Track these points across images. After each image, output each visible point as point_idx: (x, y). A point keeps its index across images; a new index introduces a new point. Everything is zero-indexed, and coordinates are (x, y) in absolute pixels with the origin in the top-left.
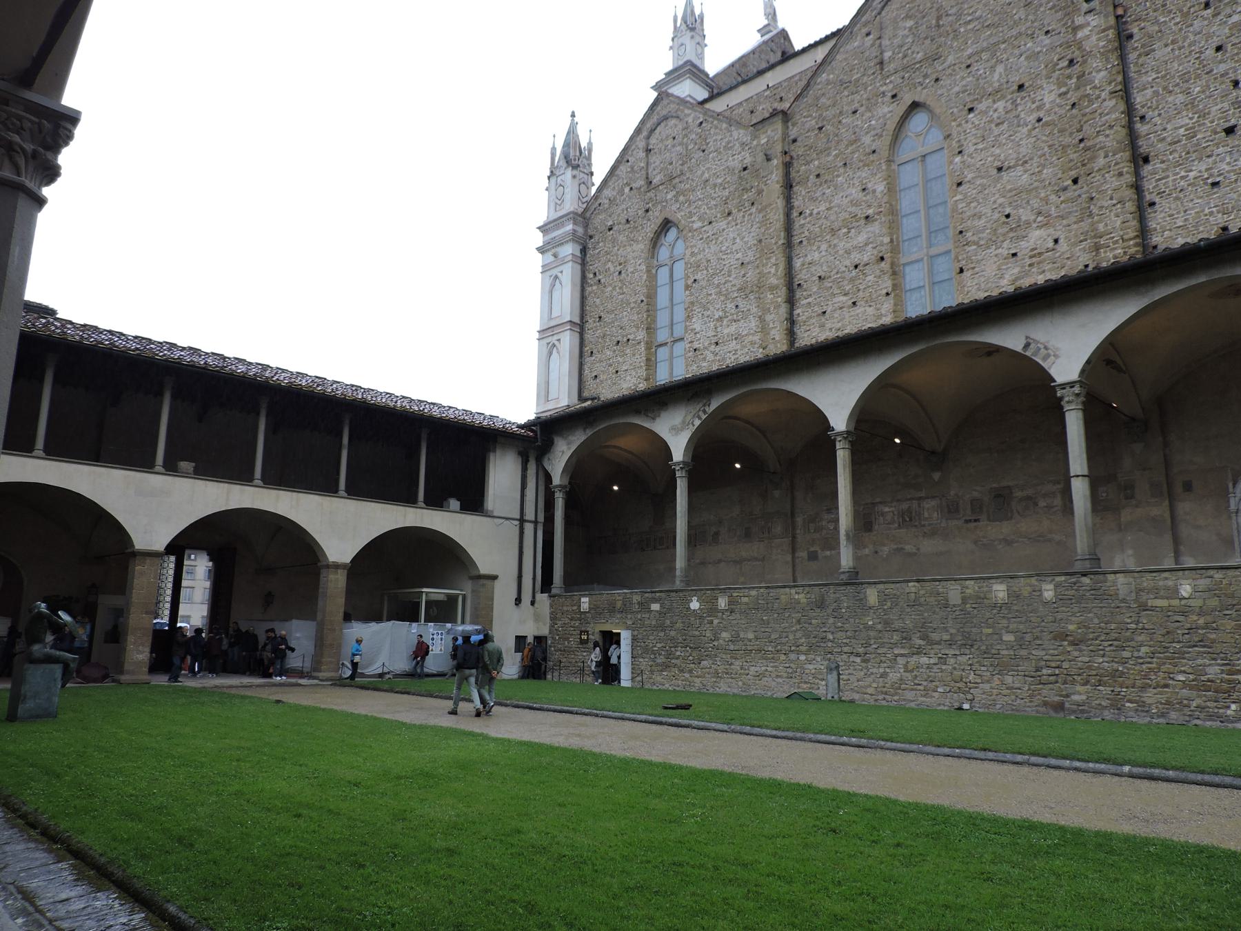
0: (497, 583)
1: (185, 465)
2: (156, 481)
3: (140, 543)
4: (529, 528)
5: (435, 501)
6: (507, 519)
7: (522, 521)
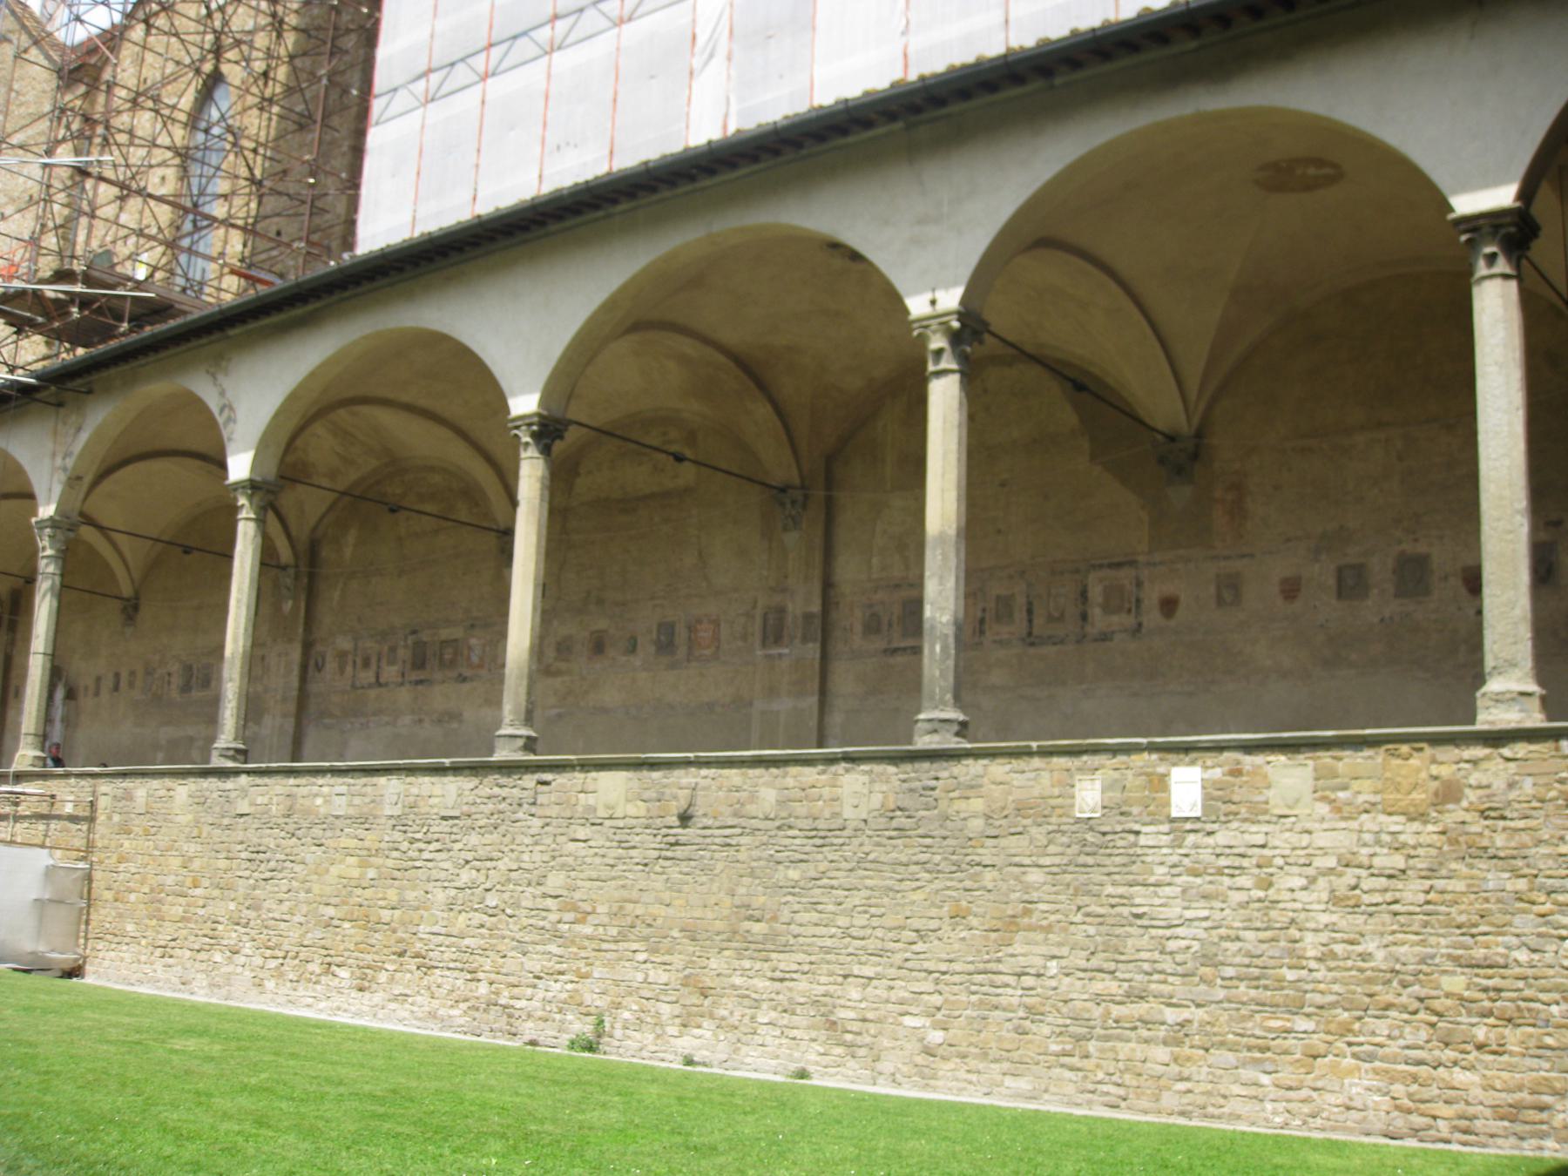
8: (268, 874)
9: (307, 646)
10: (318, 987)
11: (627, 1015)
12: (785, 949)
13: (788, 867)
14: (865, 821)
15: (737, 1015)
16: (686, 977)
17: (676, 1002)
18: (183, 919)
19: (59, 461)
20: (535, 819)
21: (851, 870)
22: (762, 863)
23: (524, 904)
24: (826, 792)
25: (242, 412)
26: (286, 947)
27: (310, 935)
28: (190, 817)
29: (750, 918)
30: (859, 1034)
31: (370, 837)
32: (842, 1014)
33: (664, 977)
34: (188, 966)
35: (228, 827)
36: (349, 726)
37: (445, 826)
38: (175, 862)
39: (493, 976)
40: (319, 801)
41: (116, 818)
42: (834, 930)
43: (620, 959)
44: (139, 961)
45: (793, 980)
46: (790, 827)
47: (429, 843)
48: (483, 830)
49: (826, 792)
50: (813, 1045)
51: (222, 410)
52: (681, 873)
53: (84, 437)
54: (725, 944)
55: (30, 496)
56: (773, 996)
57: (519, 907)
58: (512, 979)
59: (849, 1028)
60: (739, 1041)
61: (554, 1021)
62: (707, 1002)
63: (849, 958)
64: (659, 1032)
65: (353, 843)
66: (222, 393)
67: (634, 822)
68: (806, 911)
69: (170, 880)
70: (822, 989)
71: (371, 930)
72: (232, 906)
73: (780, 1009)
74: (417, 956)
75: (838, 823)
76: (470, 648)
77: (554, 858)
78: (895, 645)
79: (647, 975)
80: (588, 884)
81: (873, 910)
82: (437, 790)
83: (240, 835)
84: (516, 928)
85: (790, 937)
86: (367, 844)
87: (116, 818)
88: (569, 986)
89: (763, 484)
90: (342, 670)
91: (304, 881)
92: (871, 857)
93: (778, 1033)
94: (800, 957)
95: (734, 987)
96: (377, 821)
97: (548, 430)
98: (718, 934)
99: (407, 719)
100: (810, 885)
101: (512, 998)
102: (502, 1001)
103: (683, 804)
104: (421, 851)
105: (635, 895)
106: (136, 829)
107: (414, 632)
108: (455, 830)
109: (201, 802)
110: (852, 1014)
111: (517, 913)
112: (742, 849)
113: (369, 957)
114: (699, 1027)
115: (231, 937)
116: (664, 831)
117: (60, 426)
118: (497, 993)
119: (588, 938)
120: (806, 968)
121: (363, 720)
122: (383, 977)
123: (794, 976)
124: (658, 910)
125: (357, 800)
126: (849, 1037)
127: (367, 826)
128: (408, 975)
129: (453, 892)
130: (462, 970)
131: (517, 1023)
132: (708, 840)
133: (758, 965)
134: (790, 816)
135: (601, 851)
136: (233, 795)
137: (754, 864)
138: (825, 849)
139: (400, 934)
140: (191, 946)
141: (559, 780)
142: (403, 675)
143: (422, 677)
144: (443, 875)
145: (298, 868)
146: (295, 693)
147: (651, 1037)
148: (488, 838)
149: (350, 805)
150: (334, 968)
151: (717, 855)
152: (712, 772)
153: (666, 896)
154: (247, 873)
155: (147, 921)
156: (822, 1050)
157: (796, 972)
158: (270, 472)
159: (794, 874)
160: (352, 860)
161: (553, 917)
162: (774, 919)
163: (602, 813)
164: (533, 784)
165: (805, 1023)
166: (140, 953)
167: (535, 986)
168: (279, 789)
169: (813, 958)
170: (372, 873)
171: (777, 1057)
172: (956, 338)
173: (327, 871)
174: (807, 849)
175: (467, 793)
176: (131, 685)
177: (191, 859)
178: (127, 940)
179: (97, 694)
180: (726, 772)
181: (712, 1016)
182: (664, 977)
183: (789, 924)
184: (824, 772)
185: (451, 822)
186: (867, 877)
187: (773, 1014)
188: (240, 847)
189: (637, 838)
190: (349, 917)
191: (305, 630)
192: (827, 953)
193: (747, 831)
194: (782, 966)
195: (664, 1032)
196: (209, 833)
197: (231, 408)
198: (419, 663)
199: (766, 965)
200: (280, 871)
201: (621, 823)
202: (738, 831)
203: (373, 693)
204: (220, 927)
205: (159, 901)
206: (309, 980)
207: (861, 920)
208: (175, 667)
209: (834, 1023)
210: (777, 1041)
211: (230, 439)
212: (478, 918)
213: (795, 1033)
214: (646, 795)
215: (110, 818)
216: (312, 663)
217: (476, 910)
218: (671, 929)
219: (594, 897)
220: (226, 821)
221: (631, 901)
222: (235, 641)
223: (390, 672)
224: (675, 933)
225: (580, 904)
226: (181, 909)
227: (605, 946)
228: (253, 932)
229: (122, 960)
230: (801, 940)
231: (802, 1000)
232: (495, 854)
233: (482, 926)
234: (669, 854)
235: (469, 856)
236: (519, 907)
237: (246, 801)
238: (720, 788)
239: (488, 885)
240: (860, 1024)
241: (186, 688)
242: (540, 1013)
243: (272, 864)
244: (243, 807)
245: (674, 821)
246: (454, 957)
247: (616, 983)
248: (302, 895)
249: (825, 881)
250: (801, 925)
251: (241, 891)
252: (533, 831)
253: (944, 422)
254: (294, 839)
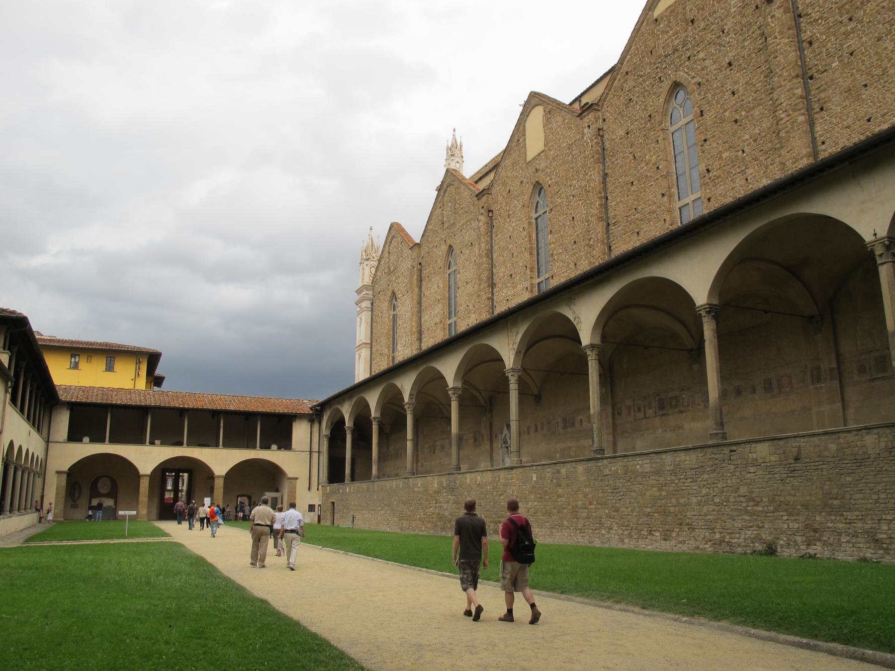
0: (297, 481)
1: (157, 442)
2: (146, 449)
3: (142, 472)
4: (315, 456)
5: (266, 446)
6: (303, 451)
7: (311, 452)
8: (620, 498)
9: (613, 406)
10: (647, 540)
11: (782, 542)
12: (850, 510)
13: (846, 476)
14: (879, 454)
15: (832, 539)
16: (807, 525)
17: (804, 535)
18: (587, 518)
19: (511, 347)
20: (731, 466)
21: (876, 475)
22: (834, 475)
23: (731, 500)
24: (859, 443)
25: (583, 318)
26: (631, 525)
27: (641, 520)
28: (585, 478)
29: (832, 498)
30: (890, 544)
31: (662, 480)
32: (880, 536)
33: (796, 526)
34: (591, 536)
35: (601, 480)
36: (635, 436)
37: (693, 472)
38: (581, 496)
39: (721, 530)
40: (638, 467)
41: (554, 481)
42: (871, 501)
43: (776, 519)
44: (571, 536)
45: (855, 523)
46: (845, 459)
47: (687, 479)
48: (709, 472)
49: (859, 443)
50: (869, 550)
51: (575, 319)
52: (798, 482)
53: (520, 336)
54: (822, 510)
55: (501, 360)
56: (847, 530)
57: (729, 502)
58: (729, 531)
59: (884, 542)
60: (834, 550)
61: (750, 546)
62: (817, 535)
63: (880, 512)
64: (797, 548)
65: (654, 482)
66: (574, 313)
67: (774, 463)
68: (857, 493)
69: (580, 503)
70: (869, 526)
71: (667, 516)
72: (607, 511)
73: (851, 536)
74: (688, 524)
75: (867, 456)
76: (683, 399)
77: (741, 481)
78: (874, 377)
79: (789, 525)
80: (758, 490)
81: (888, 491)
82: (688, 458)
83: (607, 483)
84: (729, 510)
85: (851, 505)
86: (661, 482)
87: (554, 481)
88: (755, 532)
89: (803, 316)
90: (629, 413)
91: (636, 499)
92: (884, 469)
93: (851, 545)
94: (857, 513)
95: (828, 527)
96: (664, 472)
97: (714, 311)
98: (818, 506)
99: (660, 431)
100: (858, 483)
101: (731, 538)
102: (726, 540)
103: (795, 454)
104: (684, 483)
105: (779, 493)
106: (563, 485)
107: (658, 395)
108: (697, 473)
109: (588, 471)
110: (885, 536)
111: (728, 504)
112: (824, 470)
113: (667, 527)
114: (815, 545)
115: (608, 523)
116: (788, 466)
117: (509, 333)
118: (724, 537)
119: (760, 511)
120: (861, 517)
121: (641, 433)
122: (674, 534)
123: (855, 521)
124: (788, 498)
125: (654, 465)
126: (885, 546)
127: (659, 475)
128: (685, 533)
129: (700, 498)
130: (707, 529)
131: (734, 549)
132: (808, 468)
133: (838, 518)
134: (844, 455)
135: (762, 476)
136: (602, 468)
137: (830, 476)
138: (861, 467)
139: (679, 516)
140: (591, 528)
141: (739, 449)
142: (656, 413)
143: (664, 413)
144: (694, 491)
145: (633, 494)
146: (611, 425)
147: (794, 550)
148: (712, 475)
149: (651, 467)
150: (652, 532)
151: (813, 474)
152: (806, 439)
153: (793, 492)
154: (612, 498)
155: (572, 520)
156: (873, 552)
157: (856, 519)
158: (597, 341)
159: (849, 479)
160: (654, 489)
161: (744, 505)
162: (843, 498)
163: (760, 461)
164: (728, 452)
165: (863, 540)
166: (571, 532)
167: (740, 533)
168: (620, 463)
169: (863, 513)
170: (664, 493)
171: (853, 556)
172: (888, 248)
173: (645, 494)
174: (854, 468)
175: (700, 458)
176: (542, 429)
177: (587, 494)
178: (564, 528)
179: (529, 433)
180: (812, 439)
181: (820, 540)
182: (796, 526)
183: (850, 500)
184: (856, 435)
185: (695, 470)
186: (882, 478)
187: (848, 538)
188: (607, 488)
189: (777, 470)
190: (656, 511)
191: (612, 399)
192: (869, 511)
193: (825, 462)
194: (849, 517)
195: (800, 549)
196: (594, 484)
197: (579, 318)
198: (662, 407)
199: (842, 518)
200: (625, 496)
201: (769, 464)
202: (821, 463)
203: (644, 421)
204: (603, 520)
205: (576, 512)
206: (643, 538)
207: (883, 496)
208: (560, 420)
209: (877, 540)
210: (851, 549)
211: (580, 330)
212: (711, 508)
213: (858, 545)
214: (779, 452)
215: (552, 481)
216: (616, 412)
217: (711, 504)
218: (797, 505)
219: (761, 495)
220: (600, 478)
221: (777, 496)
222: (594, 407)
223: (650, 412)
224: (799, 507)
225: (756, 498)
226: (586, 514)
227: (768, 515)
228: (617, 521)
229: (564, 535)
230: (856, 506)
231: (861, 531)
232: (716, 482)
233: (714, 510)
234: (792, 475)
235: (705, 483)
236: (729, 502)
237: (607, 470)
238: (811, 446)
239: (714, 494)
240: (889, 540)
241: (565, 427)
242: (744, 544)
243: (622, 493)
244: (607, 472)
245: (792, 461)
246: (704, 524)
247: (776, 530)
248: (636, 505)
249: (864, 481)
250: (855, 500)
251: (610, 505)
252: (731, 471)
253: (889, 284)
254: (630, 483)
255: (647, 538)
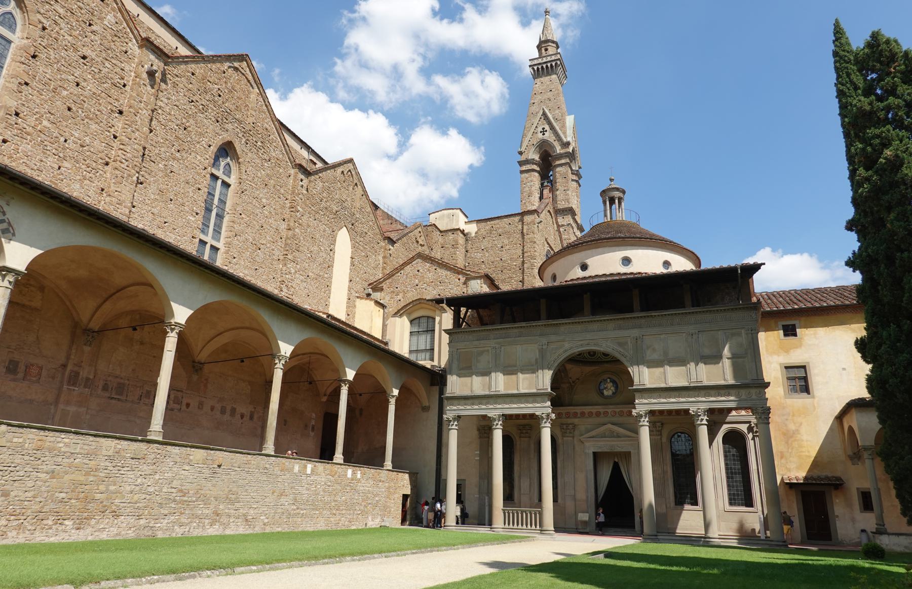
48: (149, 464)
78: (112, 396)
86: (90, 466)
94: (242, 504)
95: (226, 513)
135: (193, 474)
139: (104, 503)
161: (174, 495)
227: (190, 503)
245: (216, 466)
252: (170, 466)
255: (51, 528)
